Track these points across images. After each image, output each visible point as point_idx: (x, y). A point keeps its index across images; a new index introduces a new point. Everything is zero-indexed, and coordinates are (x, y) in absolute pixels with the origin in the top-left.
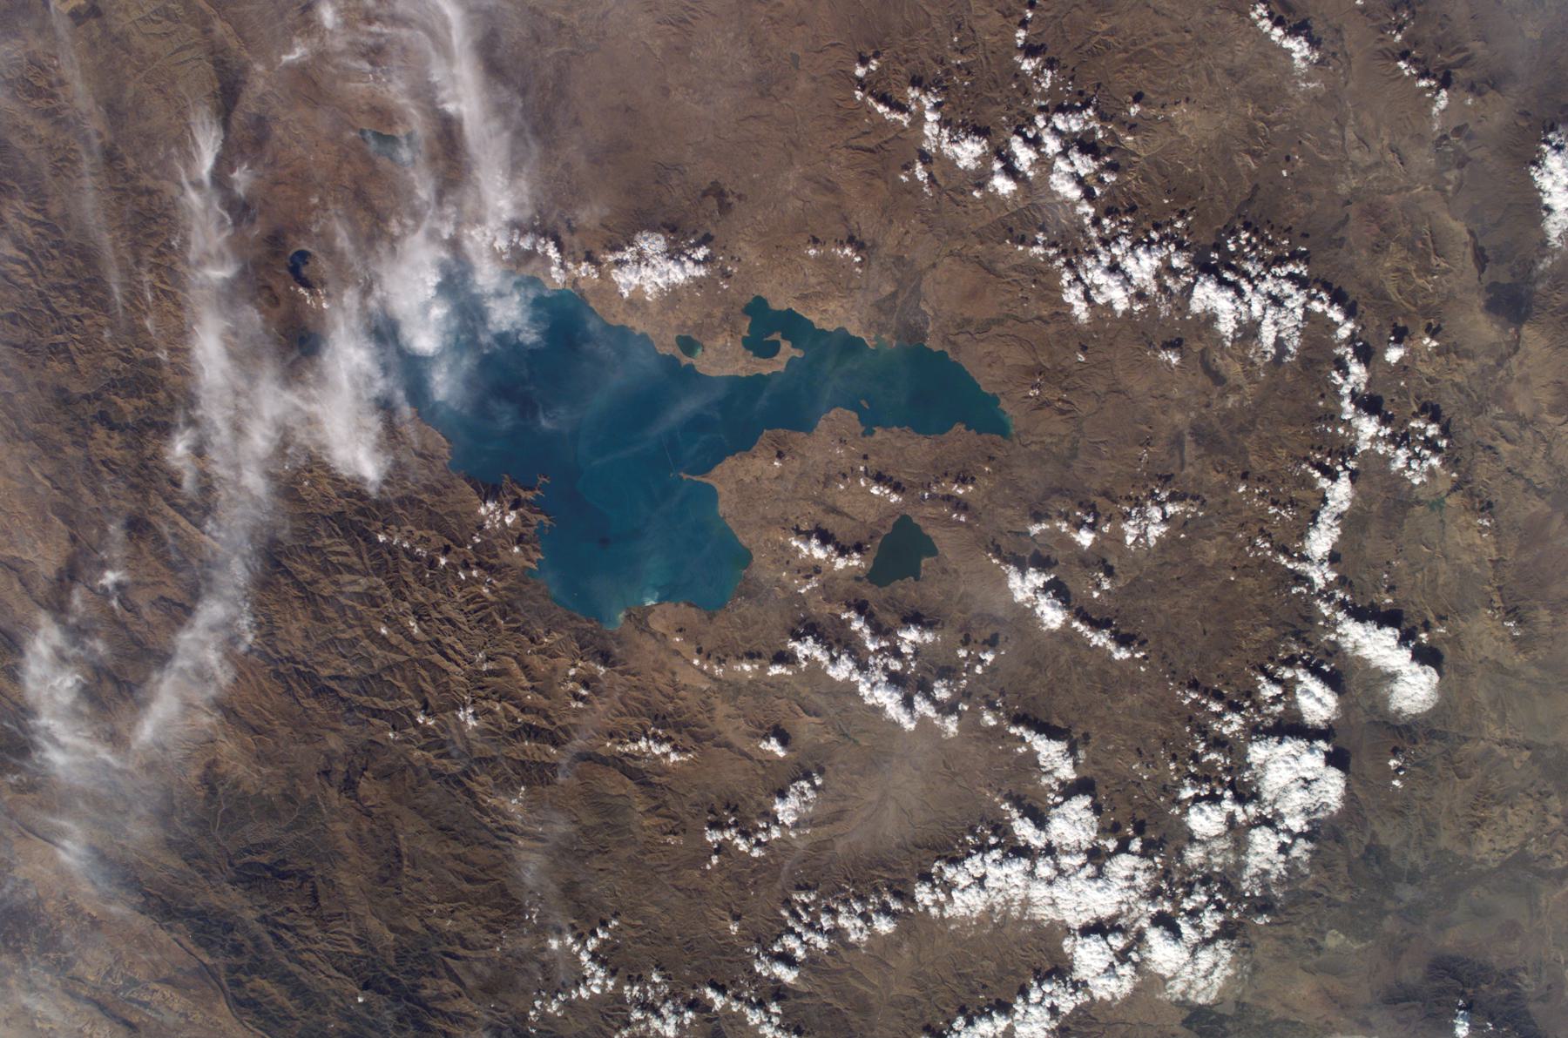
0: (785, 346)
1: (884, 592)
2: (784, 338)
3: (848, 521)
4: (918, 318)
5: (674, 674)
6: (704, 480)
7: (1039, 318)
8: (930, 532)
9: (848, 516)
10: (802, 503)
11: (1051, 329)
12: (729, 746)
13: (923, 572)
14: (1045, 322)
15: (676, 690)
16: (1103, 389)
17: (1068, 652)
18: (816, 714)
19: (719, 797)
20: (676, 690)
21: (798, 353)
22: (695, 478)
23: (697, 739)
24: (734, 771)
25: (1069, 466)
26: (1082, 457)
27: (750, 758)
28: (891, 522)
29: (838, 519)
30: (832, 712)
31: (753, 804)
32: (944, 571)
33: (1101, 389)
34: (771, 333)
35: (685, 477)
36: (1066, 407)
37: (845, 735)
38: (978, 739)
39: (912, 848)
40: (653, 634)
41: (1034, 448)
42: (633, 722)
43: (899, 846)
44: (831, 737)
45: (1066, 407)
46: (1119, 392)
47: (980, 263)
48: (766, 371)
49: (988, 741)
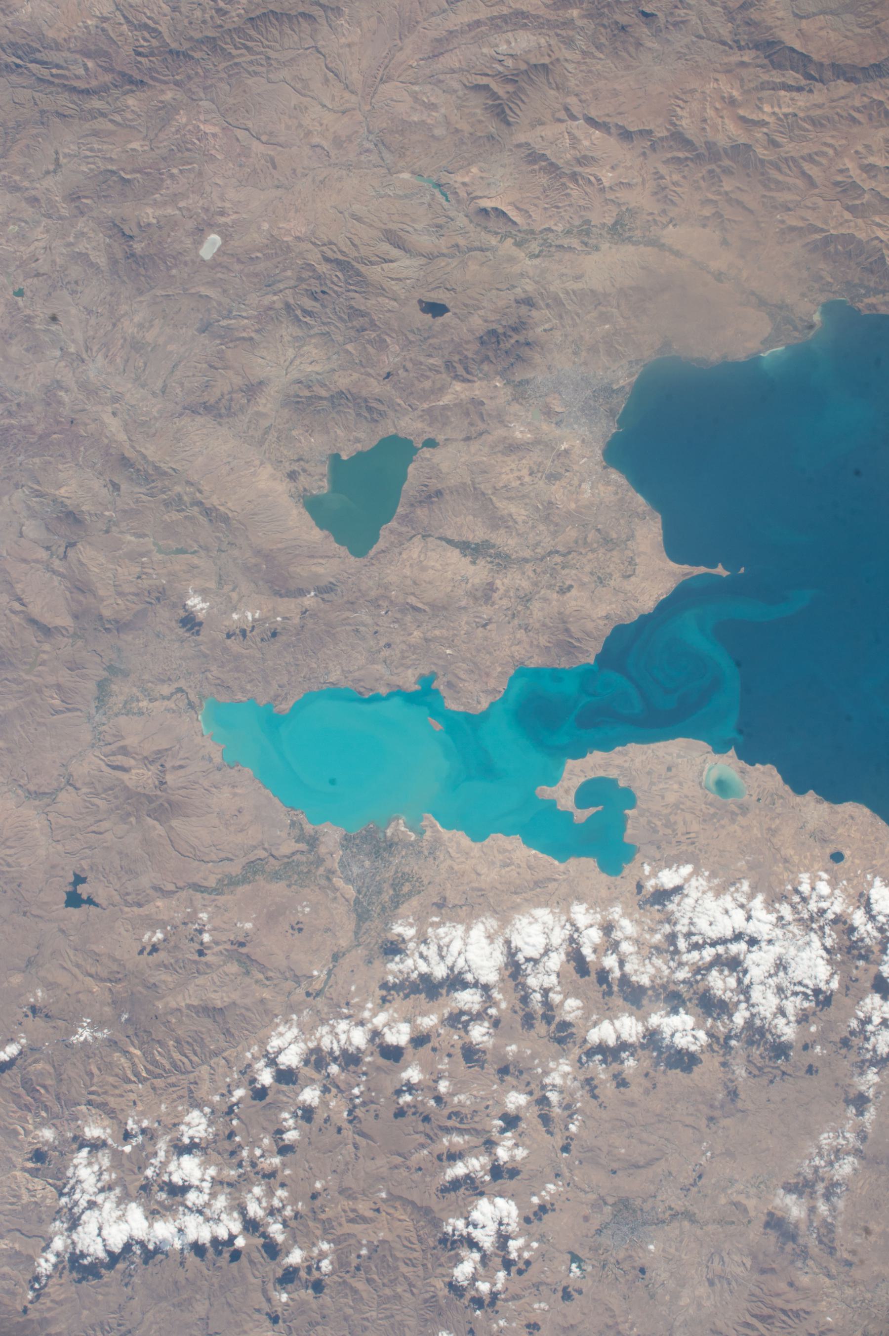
0: (567, 802)
1: (387, 428)
2: (571, 814)
3: (450, 534)
4: (356, 870)
5: (725, 243)
6: (686, 568)
7: (166, 894)
8: (316, 534)
9: (450, 542)
10: (527, 554)
11: (145, 881)
12: (626, 135)
13: (325, 469)
14: (157, 889)
15: (718, 215)
16: (63, 796)
17: (92, 375)
18: (484, 211)
19: (639, 44)
20: (718, 215)
21: (546, 792)
22: (702, 570)
23: (679, 138)
24: (615, 93)
25: (111, 669)
26: (91, 687)
27: (591, 121)
28: (381, 545)
29: (470, 537)
30: (461, 221)
31: (581, 42)
32: (292, 476)
33: (66, 797)
34: (589, 819)
35: (721, 571)
36: (120, 760)
37: (439, 185)
38: (222, 213)
39: (316, 11)
40: (762, 303)
41: (166, 690)
42: (790, 148)
43: (338, 11)
44: (459, 178)
45: (120, 760)
46: (38, 795)
47: (263, 968)
48: (596, 757)
49: (206, 210)
